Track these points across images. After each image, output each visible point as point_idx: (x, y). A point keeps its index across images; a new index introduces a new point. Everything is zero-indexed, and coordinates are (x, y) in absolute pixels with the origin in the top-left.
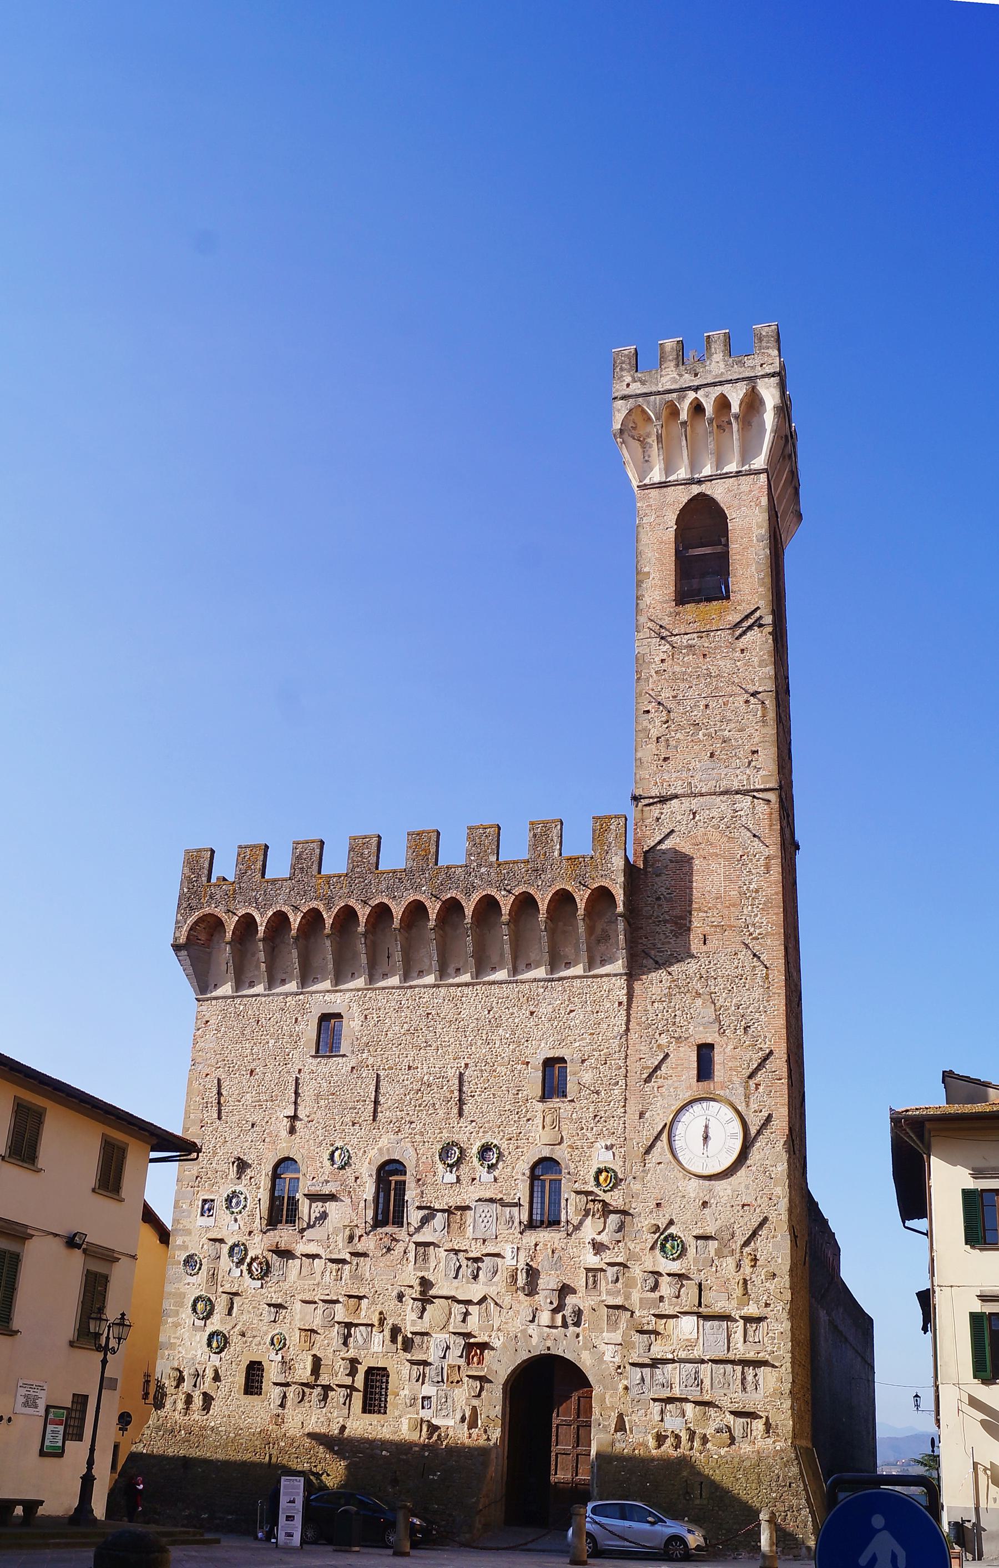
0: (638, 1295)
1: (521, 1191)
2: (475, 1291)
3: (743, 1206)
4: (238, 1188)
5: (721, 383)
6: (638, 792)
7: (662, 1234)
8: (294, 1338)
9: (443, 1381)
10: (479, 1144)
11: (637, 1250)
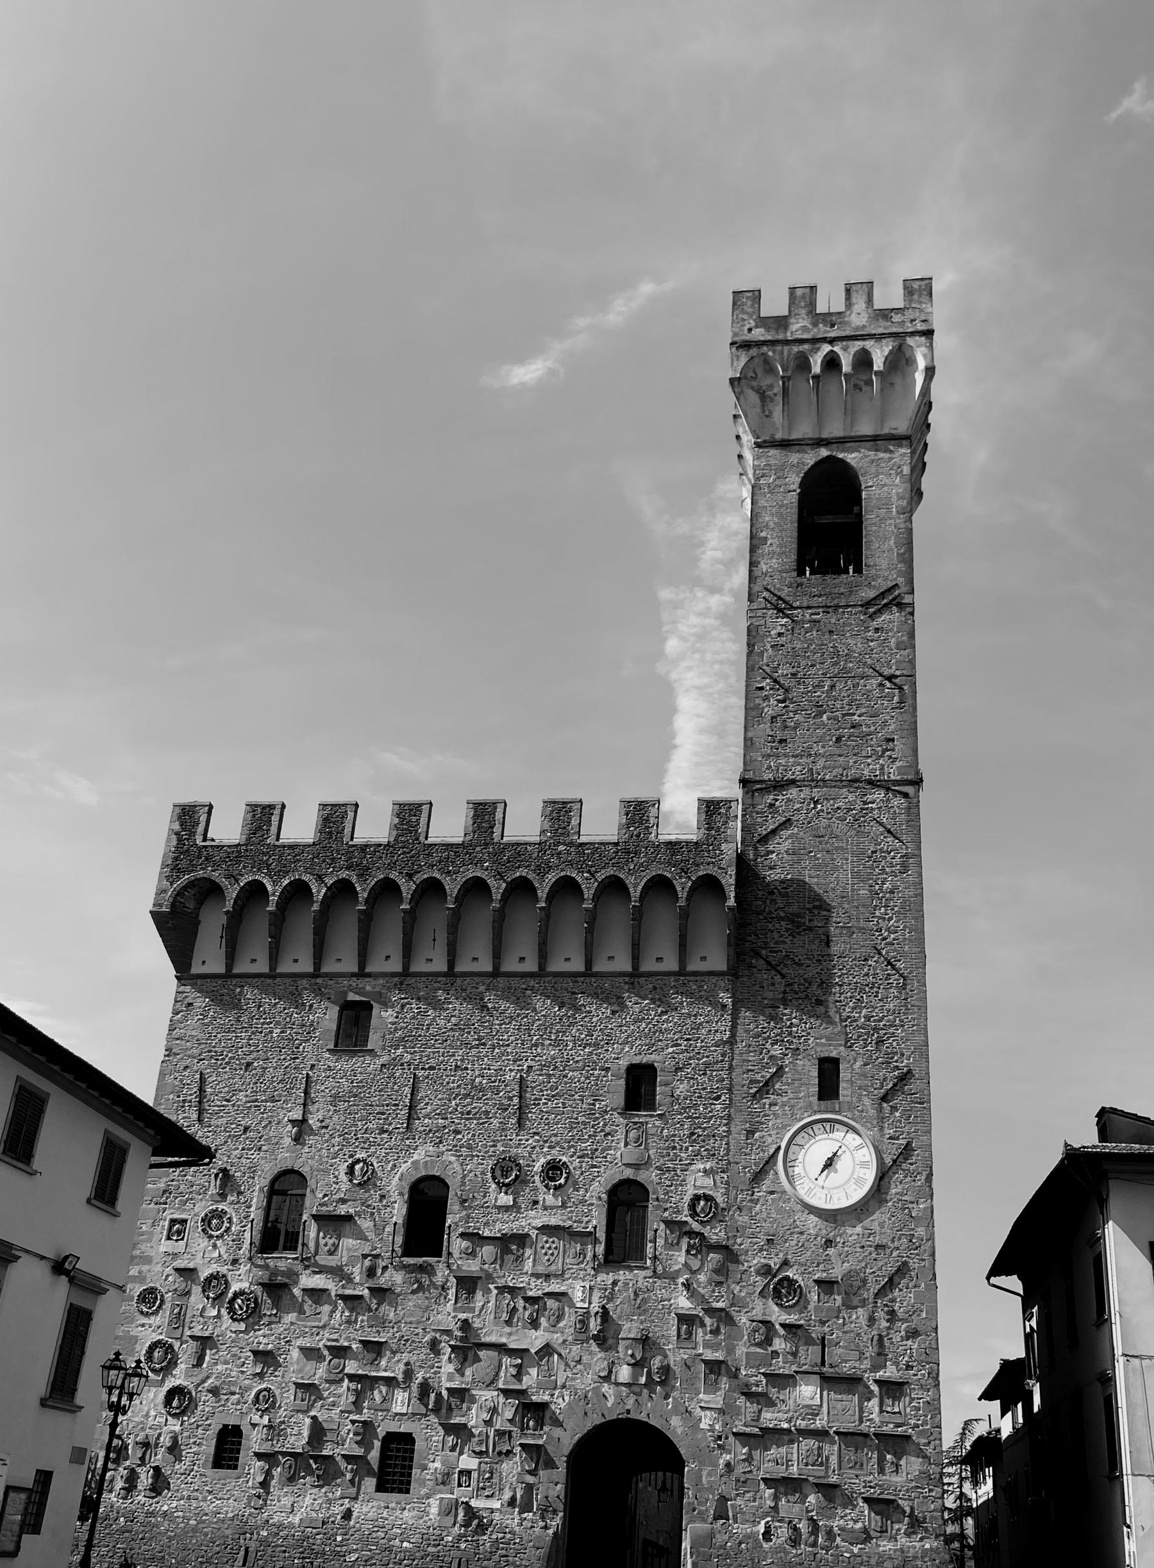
1: (597, 1220)
2: (534, 1340)
3: (878, 1247)
4: (220, 1207)
5: (863, 337)
6: (750, 775)
7: (774, 1276)
9: (487, 1452)
10: (542, 1161)
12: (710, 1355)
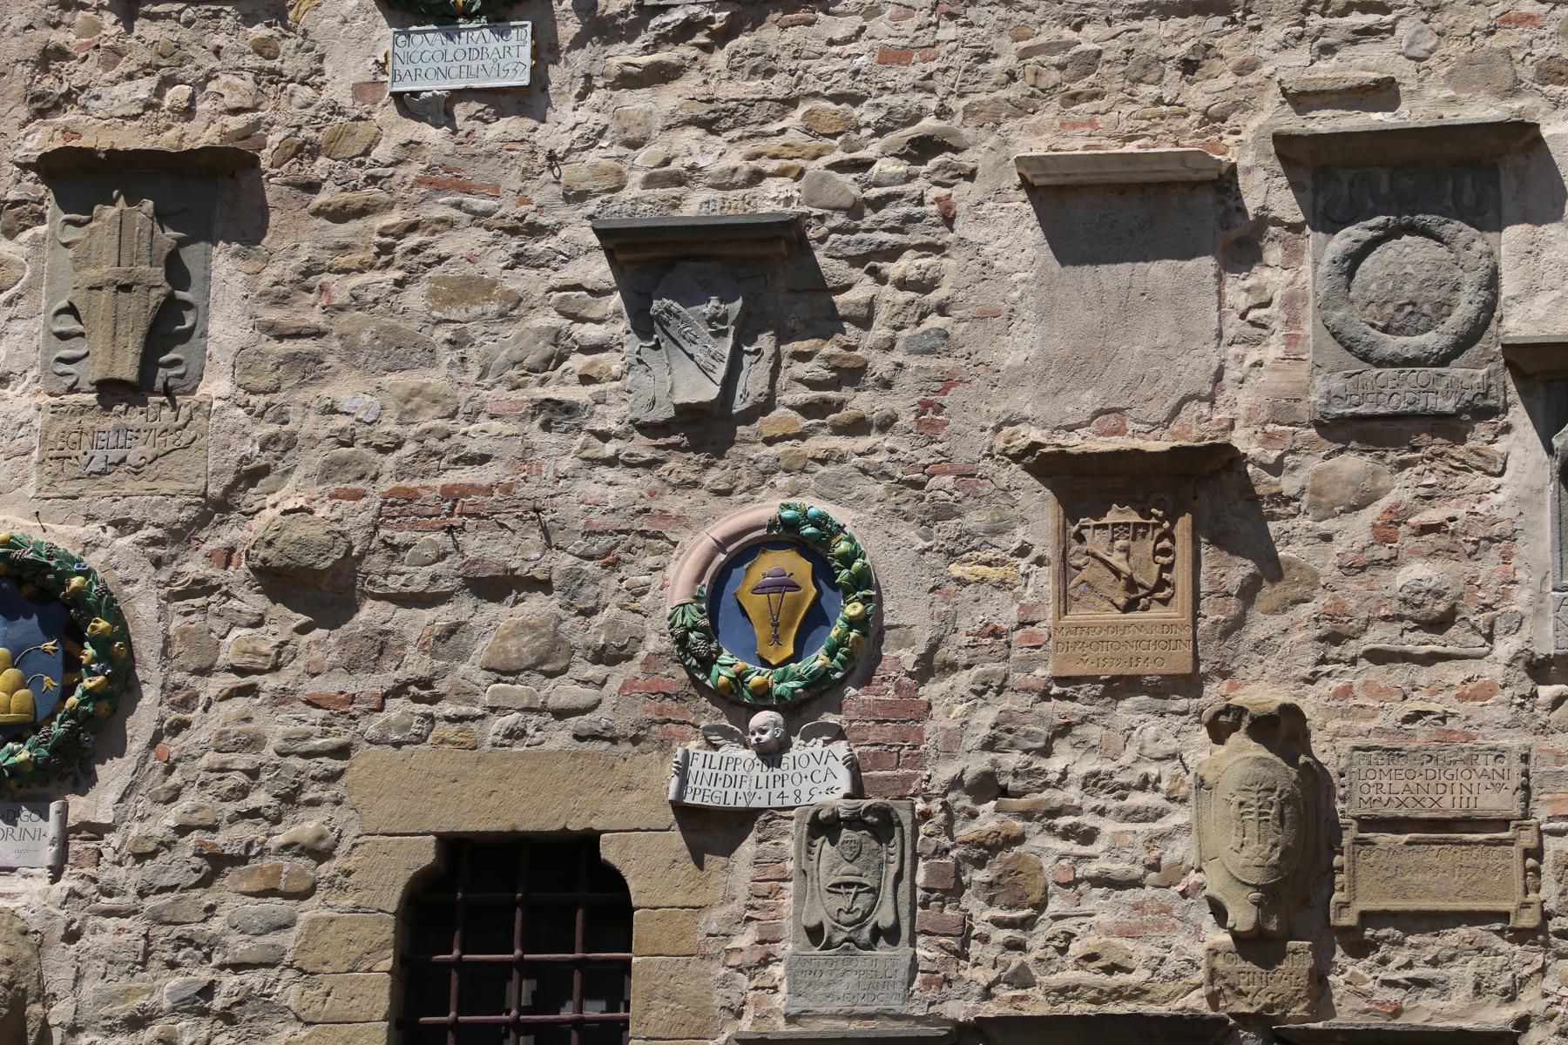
8: (980, 592)
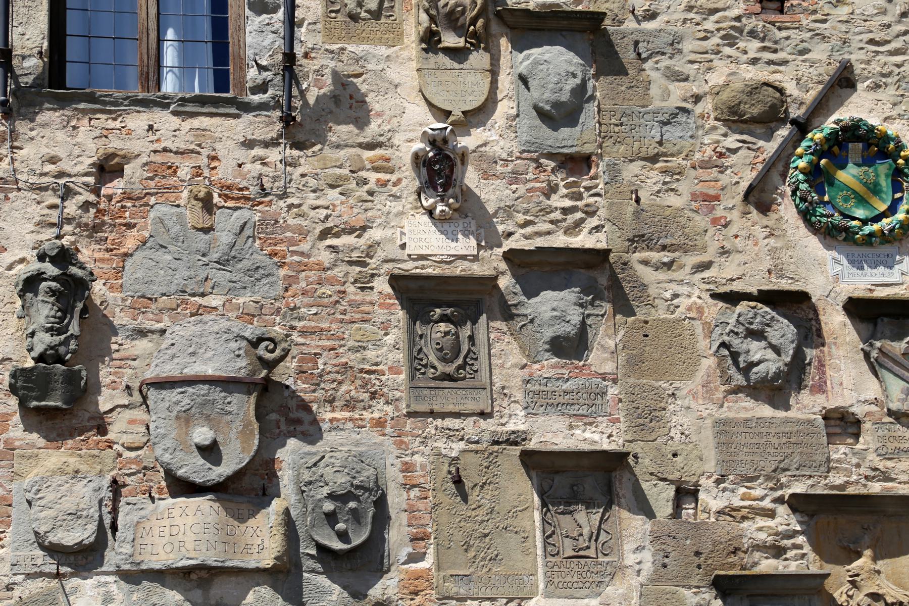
0: (710, 411)
7: (802, 128)
11: (673, 200)
12: (556, 434)
